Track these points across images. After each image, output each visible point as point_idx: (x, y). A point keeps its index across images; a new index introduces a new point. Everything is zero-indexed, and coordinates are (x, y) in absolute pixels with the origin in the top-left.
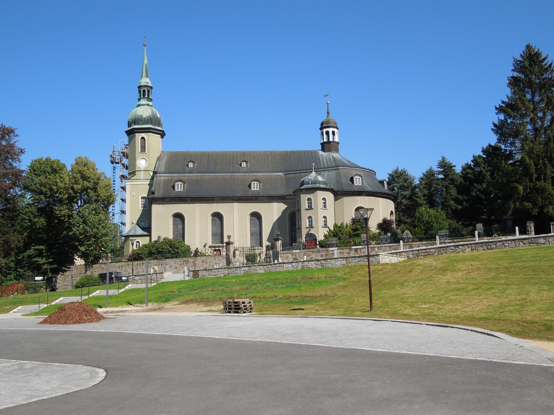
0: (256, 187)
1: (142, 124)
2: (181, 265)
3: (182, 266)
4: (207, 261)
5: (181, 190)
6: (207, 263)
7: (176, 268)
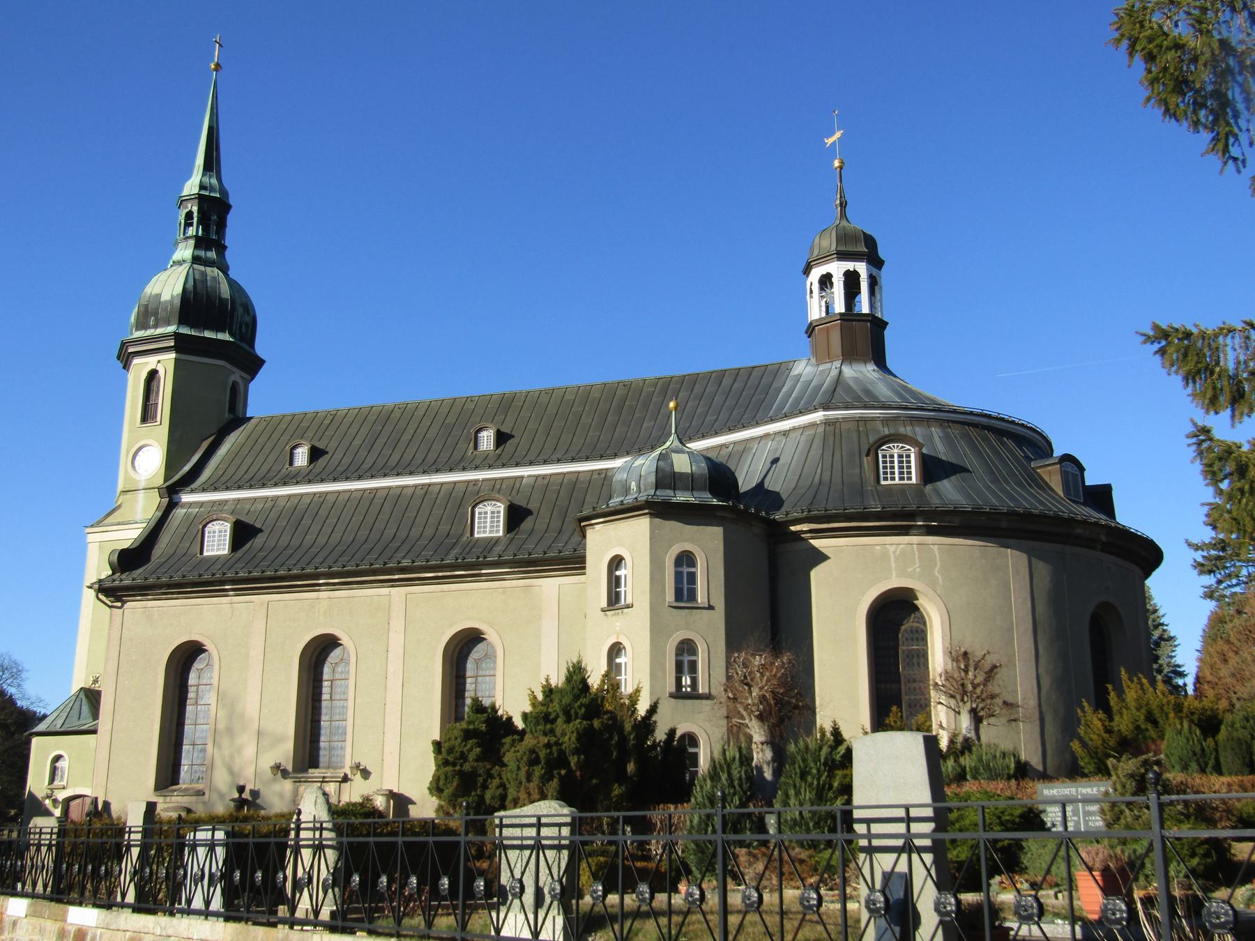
1: (156, 326)
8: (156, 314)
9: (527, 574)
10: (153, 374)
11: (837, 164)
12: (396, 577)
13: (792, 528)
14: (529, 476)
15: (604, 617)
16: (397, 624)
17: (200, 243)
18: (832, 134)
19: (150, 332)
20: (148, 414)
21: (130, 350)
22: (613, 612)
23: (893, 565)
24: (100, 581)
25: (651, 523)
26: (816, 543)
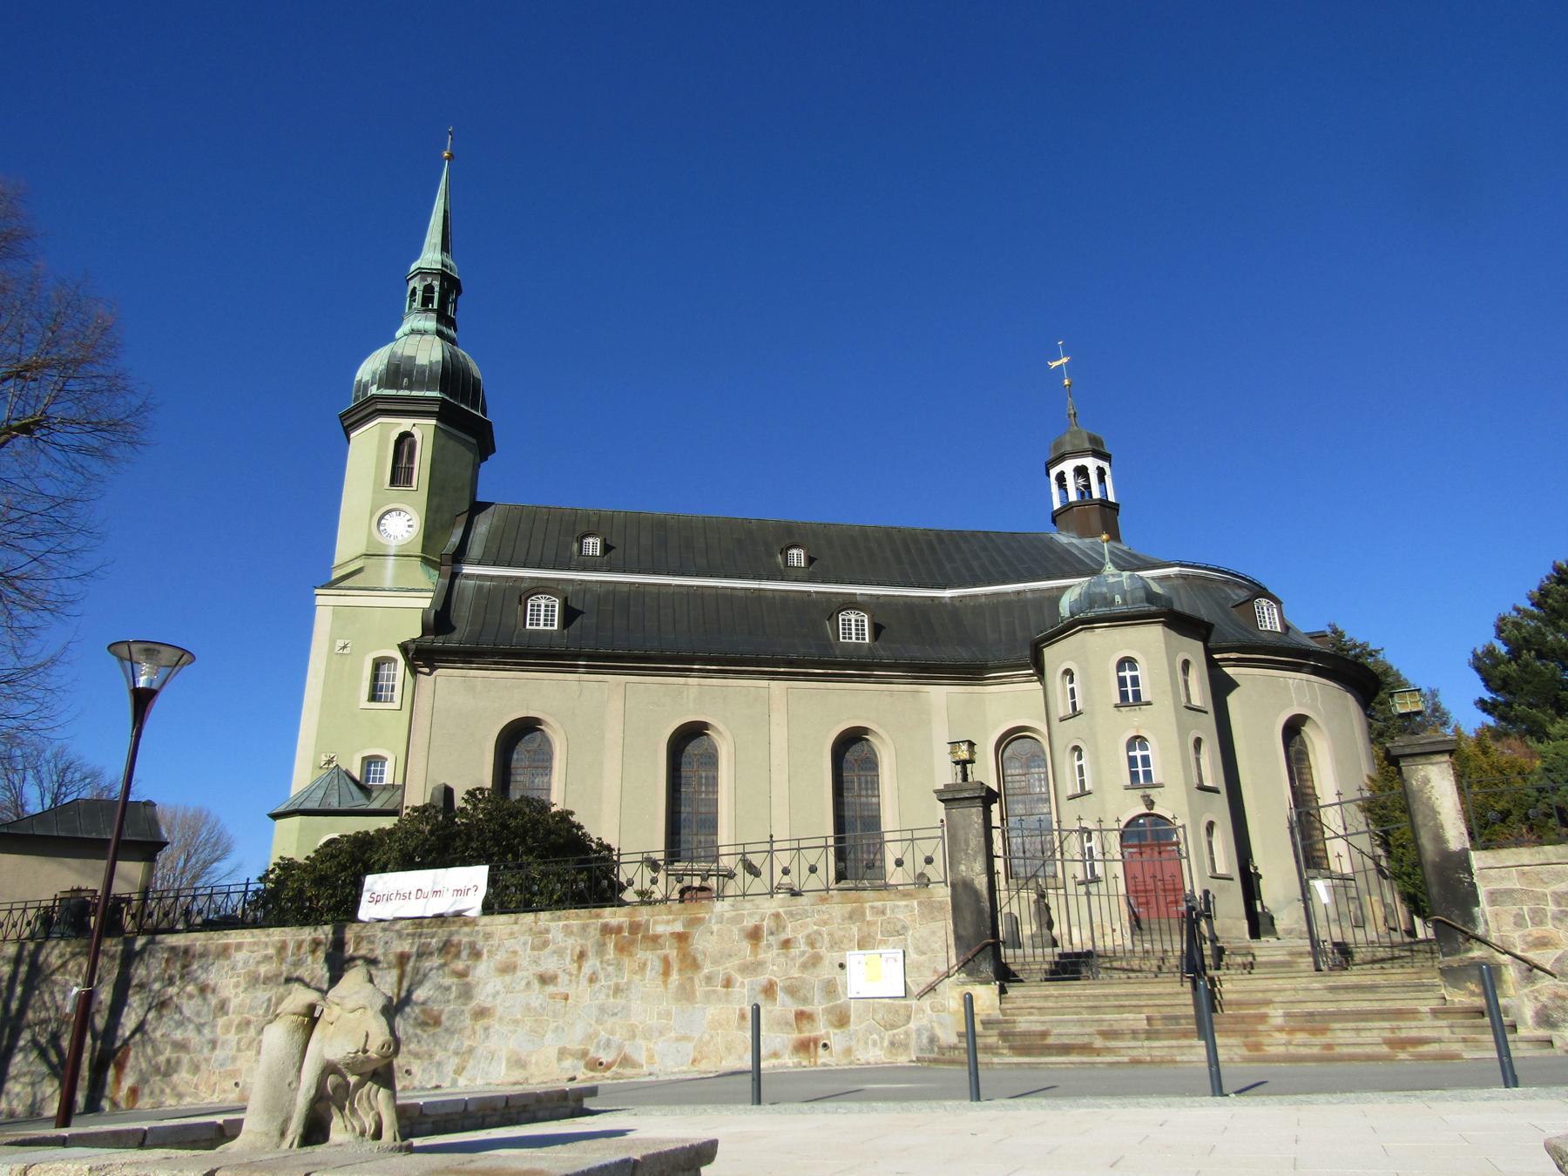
1: (410, 388)
2: (582, 955)
3: (592, 963)
5: (549, 628)
6: (786, 944)
8: (409, 374)
9: (917, 680)
10: (405, 438)
11: (1066, 382)
12: (782, 670)
13: (1216, 656)
15: (1118, 713)
16: (779, 718)
17: (443, 317)
19: (401, 393)
20: (400, 474)
21: (380, 406)
23: (1293, 695)
24: (414, 641)
25: (1164, 632)
26: (1229, 671)
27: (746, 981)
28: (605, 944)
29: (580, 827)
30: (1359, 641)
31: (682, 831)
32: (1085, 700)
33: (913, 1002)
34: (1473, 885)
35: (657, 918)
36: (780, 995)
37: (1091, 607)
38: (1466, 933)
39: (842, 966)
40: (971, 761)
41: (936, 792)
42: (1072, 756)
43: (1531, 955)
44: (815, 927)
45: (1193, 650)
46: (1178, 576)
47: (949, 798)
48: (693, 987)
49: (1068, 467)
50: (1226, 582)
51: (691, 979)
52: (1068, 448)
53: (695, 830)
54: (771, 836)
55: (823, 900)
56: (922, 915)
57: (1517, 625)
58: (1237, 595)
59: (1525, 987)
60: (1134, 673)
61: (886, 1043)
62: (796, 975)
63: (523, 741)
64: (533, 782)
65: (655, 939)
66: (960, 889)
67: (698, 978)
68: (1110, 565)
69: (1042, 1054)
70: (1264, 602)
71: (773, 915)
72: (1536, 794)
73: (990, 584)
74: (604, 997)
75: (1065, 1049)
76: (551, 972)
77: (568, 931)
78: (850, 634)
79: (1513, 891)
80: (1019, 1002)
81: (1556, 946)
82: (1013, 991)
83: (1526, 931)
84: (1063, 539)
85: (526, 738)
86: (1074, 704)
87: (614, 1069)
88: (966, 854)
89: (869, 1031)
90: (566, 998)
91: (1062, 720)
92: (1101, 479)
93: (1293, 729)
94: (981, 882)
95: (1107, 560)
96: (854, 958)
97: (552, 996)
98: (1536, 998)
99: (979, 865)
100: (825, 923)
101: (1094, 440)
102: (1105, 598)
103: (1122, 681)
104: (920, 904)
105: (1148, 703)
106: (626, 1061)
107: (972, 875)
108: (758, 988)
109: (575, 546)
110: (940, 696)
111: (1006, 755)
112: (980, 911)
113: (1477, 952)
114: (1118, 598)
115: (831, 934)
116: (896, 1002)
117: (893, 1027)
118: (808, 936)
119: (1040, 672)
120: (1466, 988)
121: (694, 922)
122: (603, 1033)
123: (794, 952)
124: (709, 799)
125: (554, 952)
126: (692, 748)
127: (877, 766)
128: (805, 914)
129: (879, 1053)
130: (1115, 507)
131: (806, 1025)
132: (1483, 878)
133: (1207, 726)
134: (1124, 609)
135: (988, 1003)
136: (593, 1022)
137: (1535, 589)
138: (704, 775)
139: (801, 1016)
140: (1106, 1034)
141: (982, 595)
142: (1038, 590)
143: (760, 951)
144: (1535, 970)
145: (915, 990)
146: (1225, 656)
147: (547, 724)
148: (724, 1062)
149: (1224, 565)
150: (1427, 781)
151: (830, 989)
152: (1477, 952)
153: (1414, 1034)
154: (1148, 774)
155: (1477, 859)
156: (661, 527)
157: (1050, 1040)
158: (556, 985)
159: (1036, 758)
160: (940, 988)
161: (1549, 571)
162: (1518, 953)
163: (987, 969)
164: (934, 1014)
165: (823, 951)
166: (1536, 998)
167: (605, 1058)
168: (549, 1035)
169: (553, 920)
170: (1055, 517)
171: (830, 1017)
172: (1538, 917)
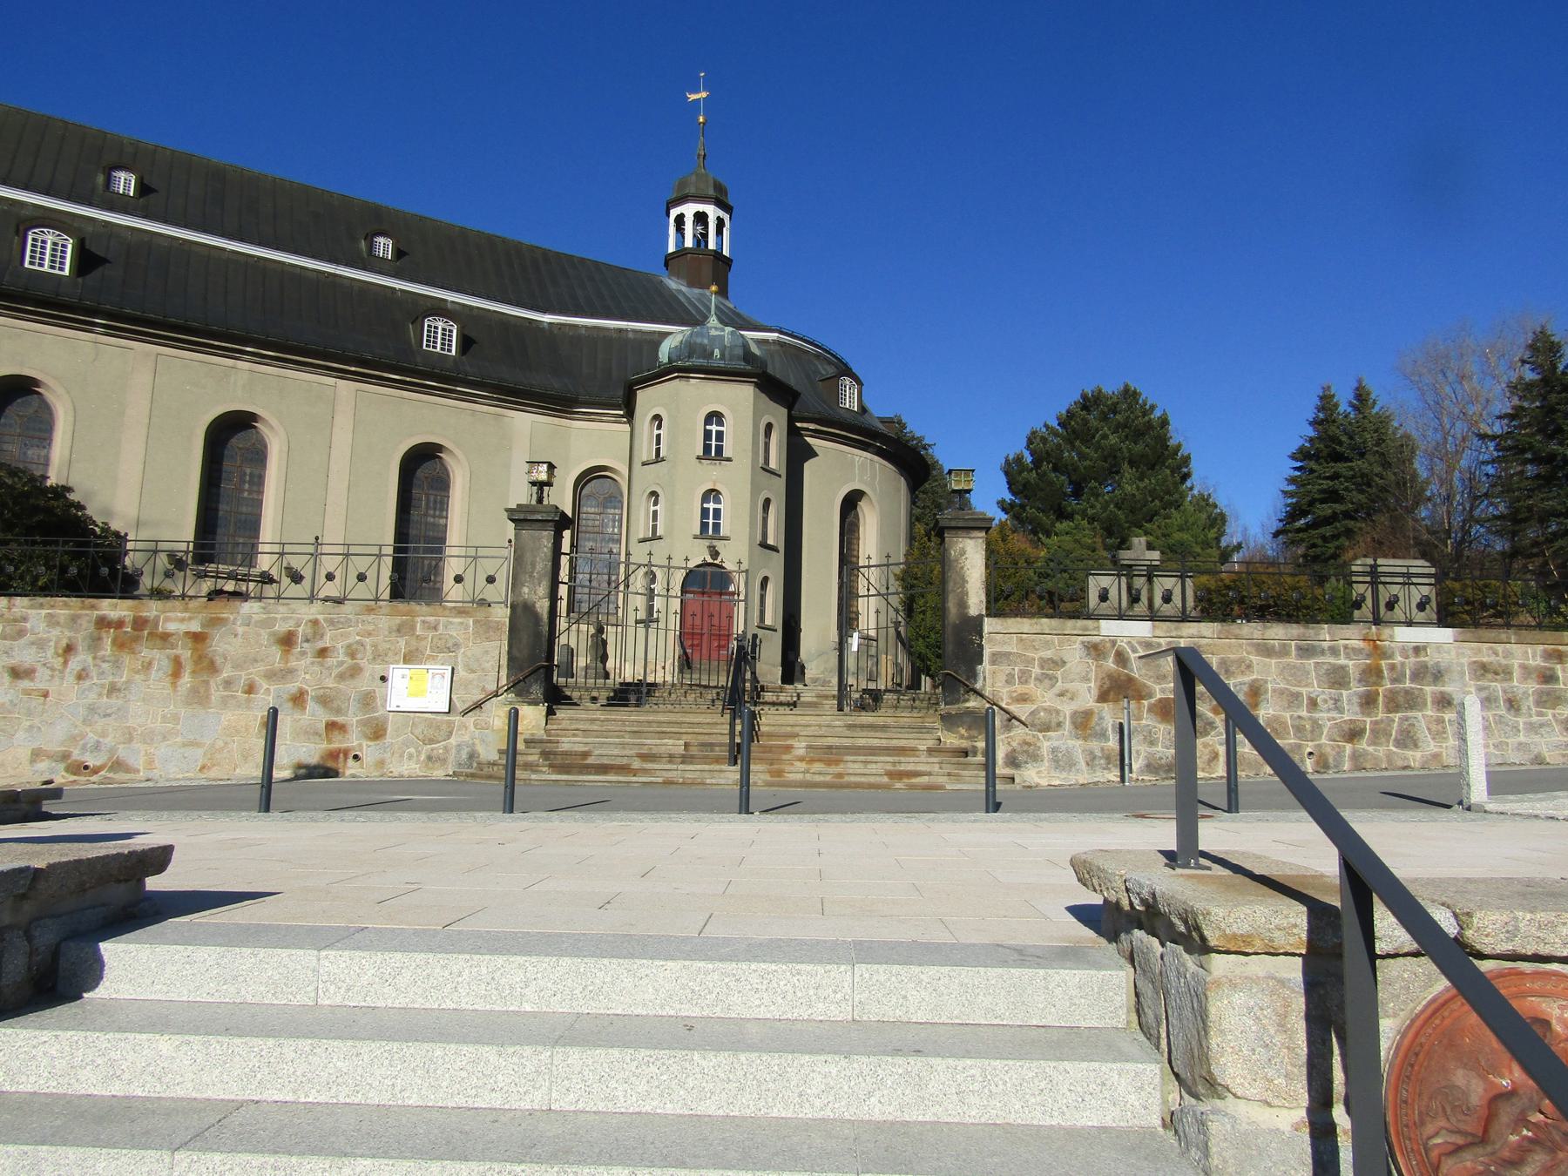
0: (439, 336)
2: (69, 649)
3: (80, 659)
4: (326, 642)
6: (323, 653)
7: (16, 673)
11: (701, 120)
12: (353, 369)
13: (798, 425)
14: (453, 302)
15: (698, 465)
18: (698, 91)
22: (709, 462)
26: (808, 439)
27: (272, 688)
28: (100, 639)
29: (80, 507)
30: (918, 434)
31: (219, 531)
32: (669, 447)
33: (457, 719)
34: (981, 646)
35: (168, 614)
36: (311, 705)
37: (690, 356)
38: (968, 686)
39: (383, 679)
40: (549, 484)
41: (507, 510)
42: (649, 501)
43: (1013, 708)
44: (358, 638)
45: (778, 415)
46: (775, 342)
47: (521, 518)
48: (208, 689)
49: (689, 210)
50: (818, 356)
51: (207, 683)
52: (692, 190)
53: (231, 531)
54: (317, 538)
55: (370, 610)
56: (476, 633)
57: (1044, 440)
58: (825, 369)
59: (1003, 734)
60: (720, 428)
61: (423, 757)
62: (331, 686)
63: (15, 404)
64: (25, 454)
65: (165, 637)
66: (519, 610)
67: (215, 682)
68: (714, 317)
69: (581, 773)
70: (847, 381)
71: (310, 621)
72: (1036, 578)
73: (592, 316)
74: (95, 696)
75: (603, 769)
76: (27, 665)
77: (52, 621)
78: (435, 342)
79: (1010, 653)
80: (565, 724)
81: (1033, 701)
82: (563, 713)
83: (1013, 688)
84: (673, 284)
85: (19, 401)
86: (658, 450)
87: (102, 773)
88: (530, 576)
89: (406, 744)
90: (46, 695)
91: (644, 464)
92: (719, 232)
93: (851, 503)
94: (543, 606)
95: (713, 312)
96: (399, 675)
97: (27, 692)
98: (1009, 743)
99: (543, 590)
100: (370, 634)
101: (719, 187)
102: (705, 350)
103: (707, 435)
104: (475, 622)
105: (729, 460)
106: (118, 765)
107: (534, 598)
108: (286, 696)
109: (101, 179)
110: (525, 424)
111: (584, 492)
112: (538, 635)
113: (973, 703)
114: (717, 352)
115: (375, 646)
116: (439, 717)
117: (432, 741)
118: (349, 646)
119: (630, 415)
120: (958, 732)
121: (215, 622)
122: (91, 735)
123: (330, 661)
124: (253, 499)
125: (33, 643)
126: (237, 442)
127: (448, 487)
128: (348, 623)
129: (414, 766)
130: (727, 262)
131: (336, 735)
132: (990, 641)
133: (777, 490)
134: (722, 364)
135: (533, 723)
136: (79, 723)
137: (1064, 412)
138: (248, 471)
139: (332, 726)
140: (644, 757)
141: (586, 327)
142: (640, 331)
143: (291, 658)
144: (1013, 721)
145: (460, 706)
146: (805, 425)
147: (47, 387)
148: (238, 771)
149: (821, 340)
150: (963, 552)
151: (368, 701)
152: (973, 703)
153: (910, 767)
154: (717, 527)
155: (989, 625)
156: (218, 176)
157: (590, 761)
158: (32, 680)
159: (613, 500)
160: (486, 706)
161: (1078, 397)
162: (1004, 706)
163: (537, 690)
164: (477, 732)
165: (363, 663)
166: (1009, 743)
167: (92, 762)
168: (21, 735)
169: (32, 607)
170: (669, 260)
171: (365, 729)
172: (1024, 677)
